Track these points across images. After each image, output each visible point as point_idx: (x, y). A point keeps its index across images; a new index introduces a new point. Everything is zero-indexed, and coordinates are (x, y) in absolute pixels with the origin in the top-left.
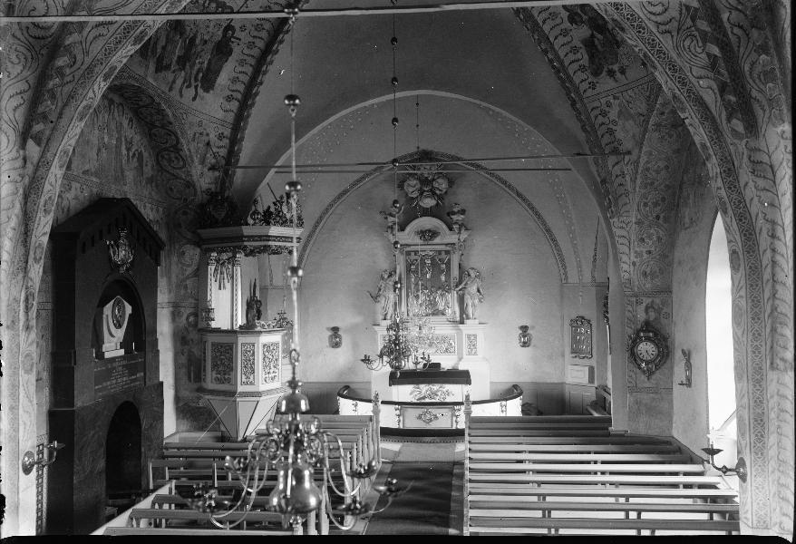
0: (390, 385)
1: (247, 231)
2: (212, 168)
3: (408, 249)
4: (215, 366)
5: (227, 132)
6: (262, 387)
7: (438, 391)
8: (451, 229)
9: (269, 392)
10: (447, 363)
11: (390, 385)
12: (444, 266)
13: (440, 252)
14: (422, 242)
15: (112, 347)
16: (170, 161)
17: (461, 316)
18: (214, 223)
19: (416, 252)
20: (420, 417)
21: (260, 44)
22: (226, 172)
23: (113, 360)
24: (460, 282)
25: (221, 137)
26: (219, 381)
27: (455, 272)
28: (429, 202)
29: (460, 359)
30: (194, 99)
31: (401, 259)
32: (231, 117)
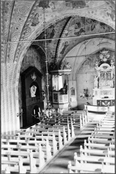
1: (59, 71)
2: (52, 58)
4: (54, 99)
5: (55, 50)
6: (64, 102)
8: (111, 66)
9: (65, 103)
12: (109, 75)
13: (108, 71)
15: (33, 95)
16: (43, 57)
18: (53, 69)
19: (102, 72)
20: (102, 109)
21: (60, 32)
22: (55, 59)
23: (33, 97)
25: (53, 51)
26: (55, 101)
28: (105, 60)
30: (47, 45)
32: (55, 47)
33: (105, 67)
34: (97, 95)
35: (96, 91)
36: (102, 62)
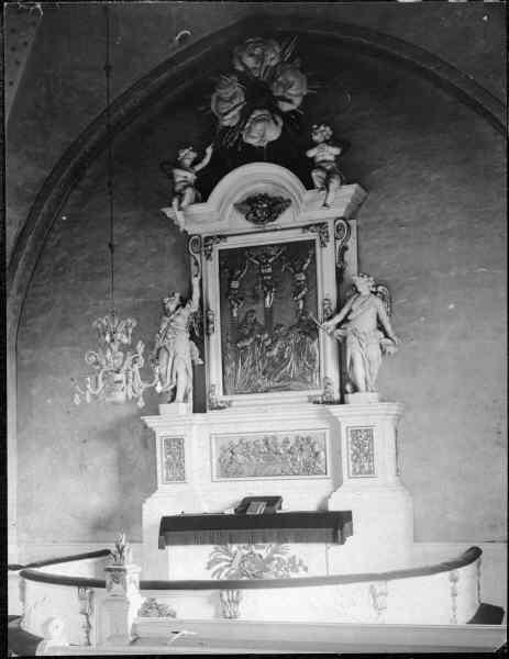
0: (161, 547)
3: (224, 245)
7: (270, 560)
8: (309, 185)
10: (299, 496)
11: (161, 547)
14: (249, 226)
17: (343, 392)
24: (338, 310)
27: (327, 288)
28: (265, 132)
29: (337, 484)
31: (212, 269)
33: (262, 208)
34: (182, 478)
35: (168, 442)
36: (235, 154)
